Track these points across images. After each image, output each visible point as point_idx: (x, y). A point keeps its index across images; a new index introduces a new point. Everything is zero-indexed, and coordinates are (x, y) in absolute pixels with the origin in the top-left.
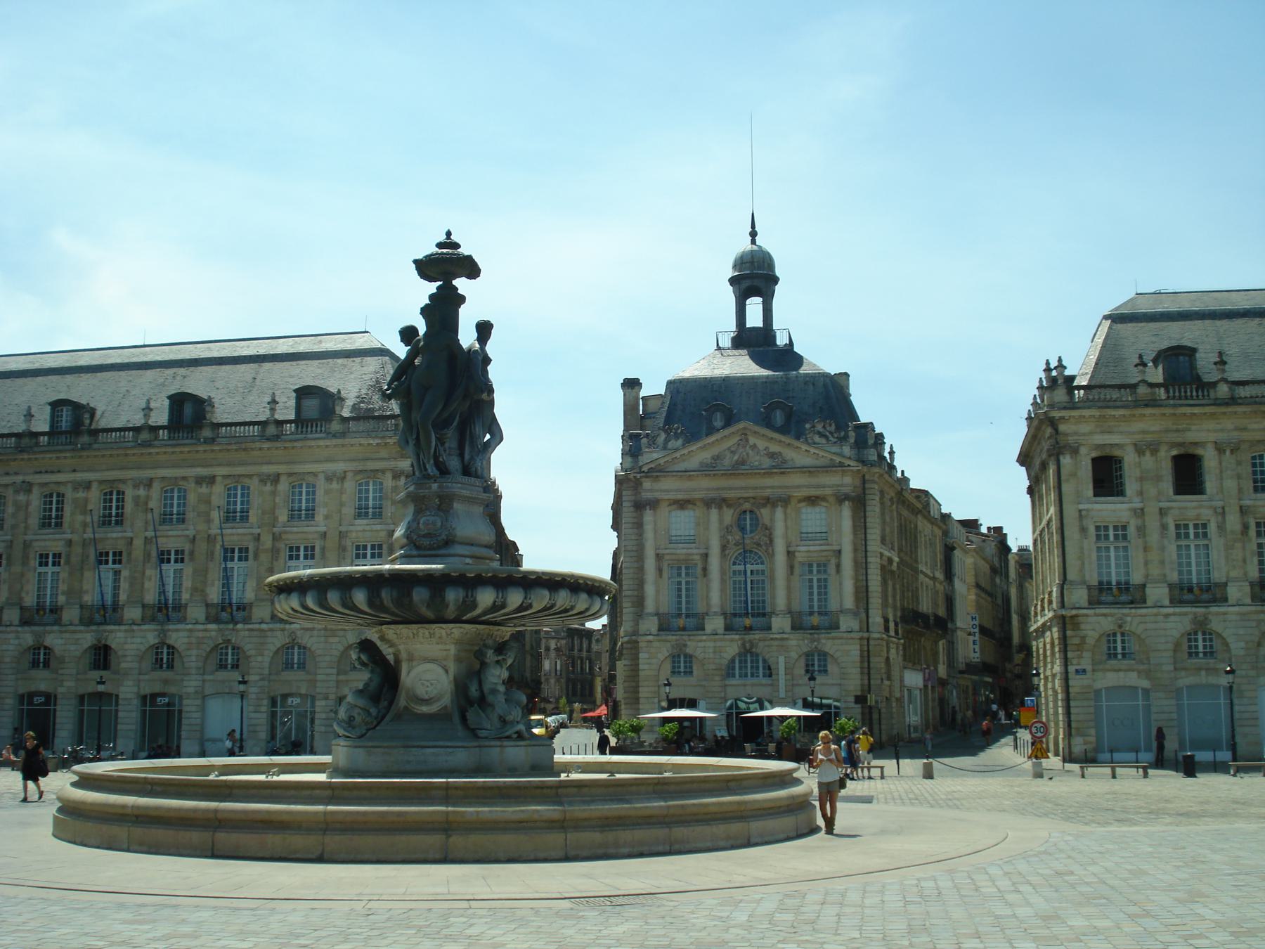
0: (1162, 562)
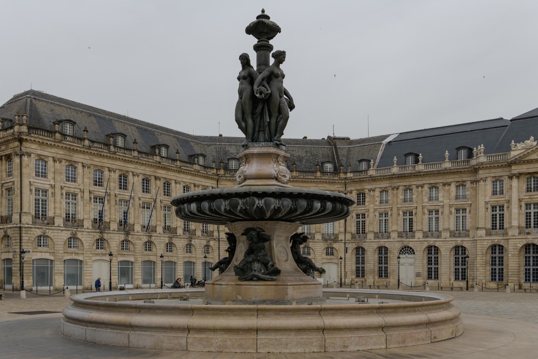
0: (61, 209)
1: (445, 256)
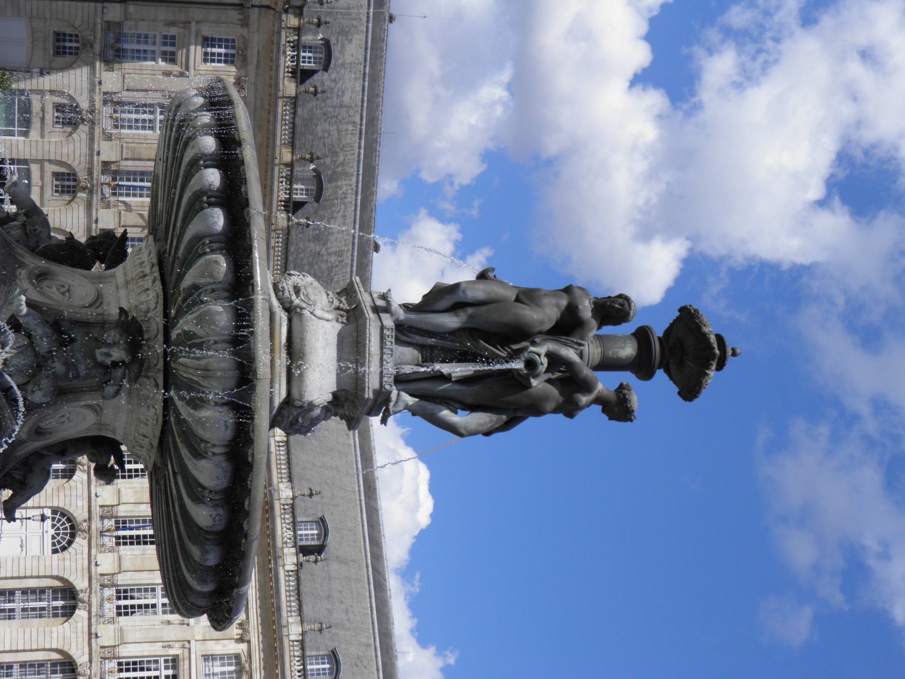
1: (48, 635)
